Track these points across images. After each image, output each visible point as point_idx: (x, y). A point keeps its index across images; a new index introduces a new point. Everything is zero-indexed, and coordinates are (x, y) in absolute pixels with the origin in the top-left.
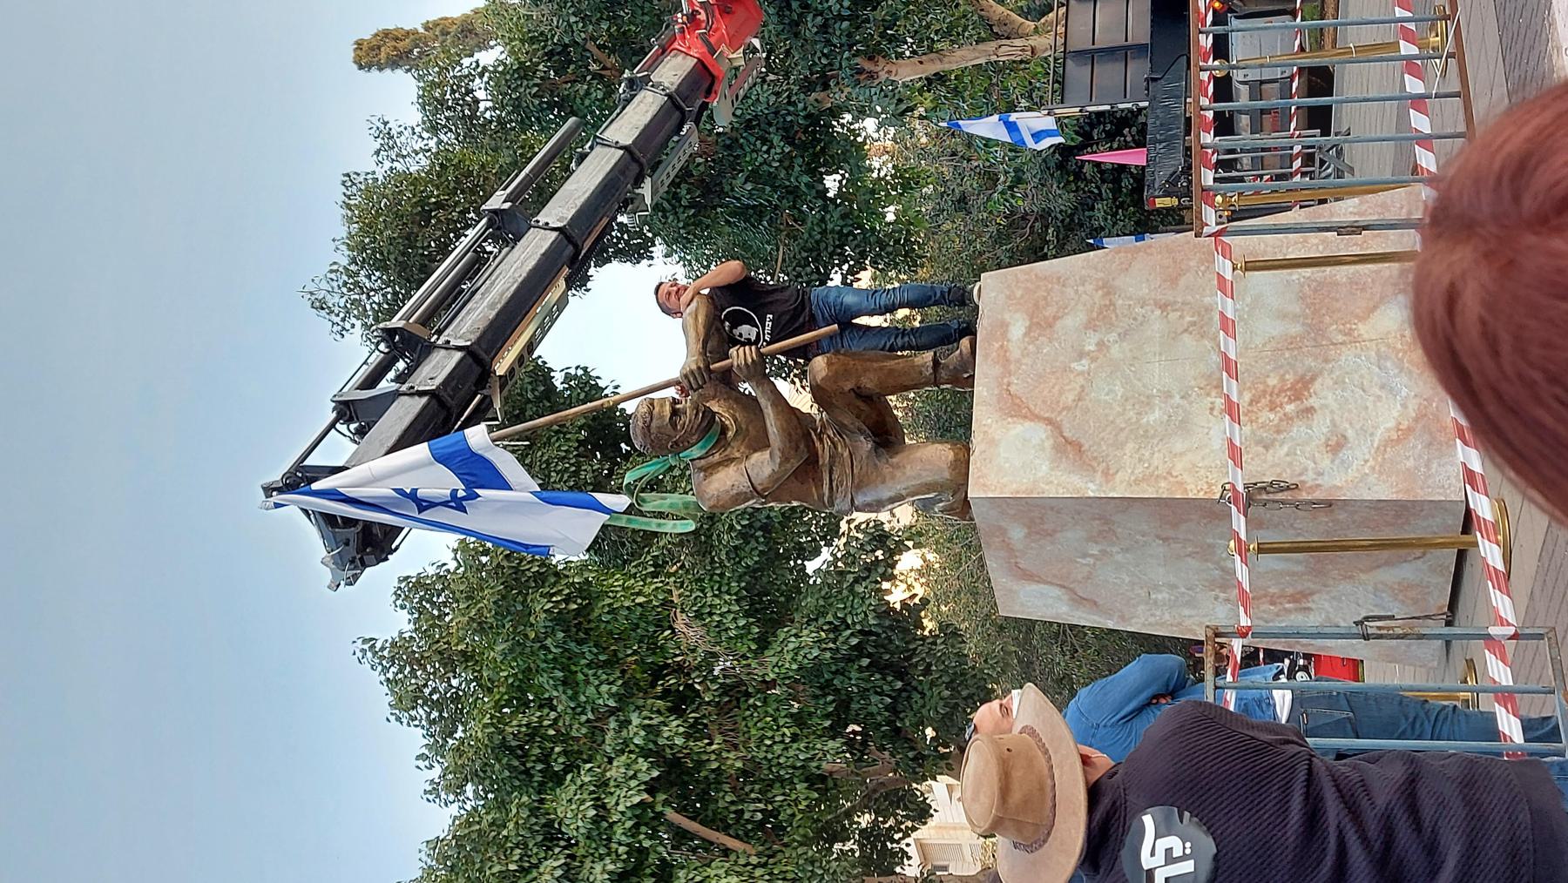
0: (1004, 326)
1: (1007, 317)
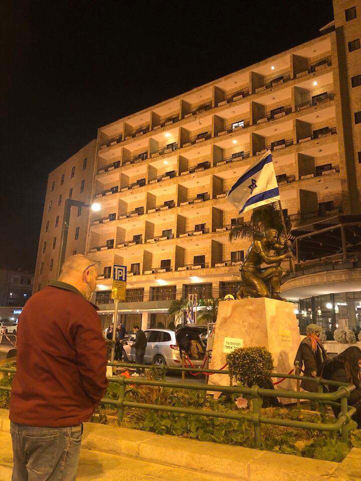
0: (251, 304)
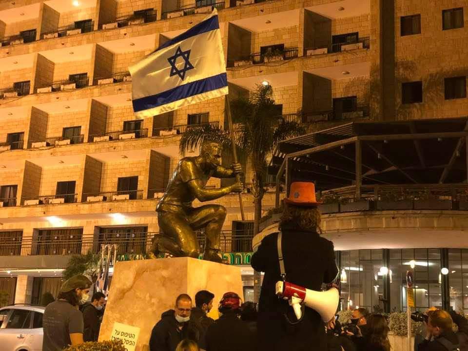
0: (166, 267)
1: (170, 269)
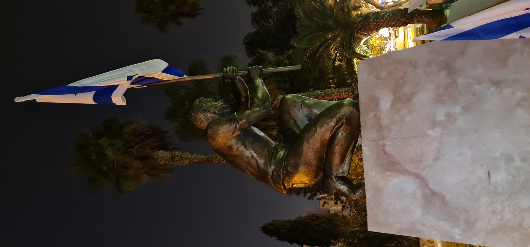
0: (375, 101)
